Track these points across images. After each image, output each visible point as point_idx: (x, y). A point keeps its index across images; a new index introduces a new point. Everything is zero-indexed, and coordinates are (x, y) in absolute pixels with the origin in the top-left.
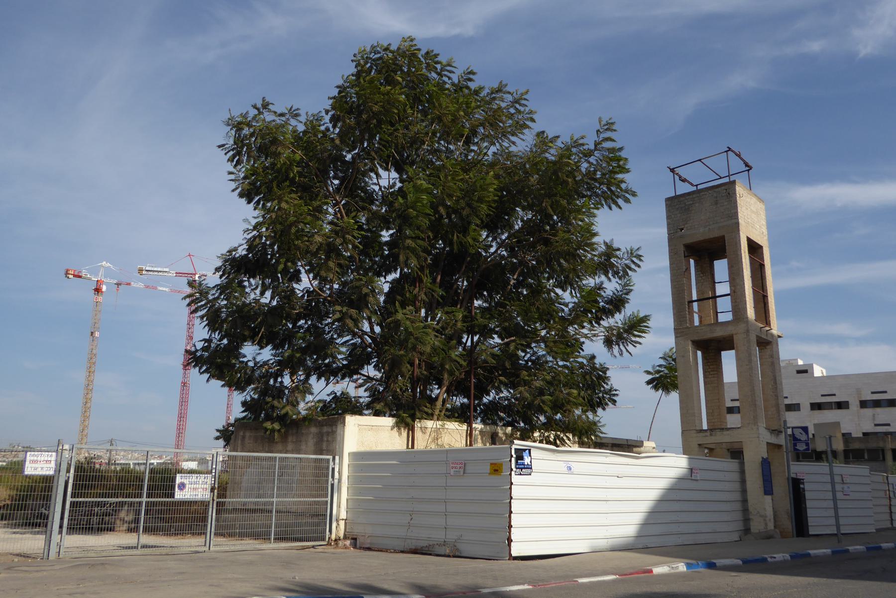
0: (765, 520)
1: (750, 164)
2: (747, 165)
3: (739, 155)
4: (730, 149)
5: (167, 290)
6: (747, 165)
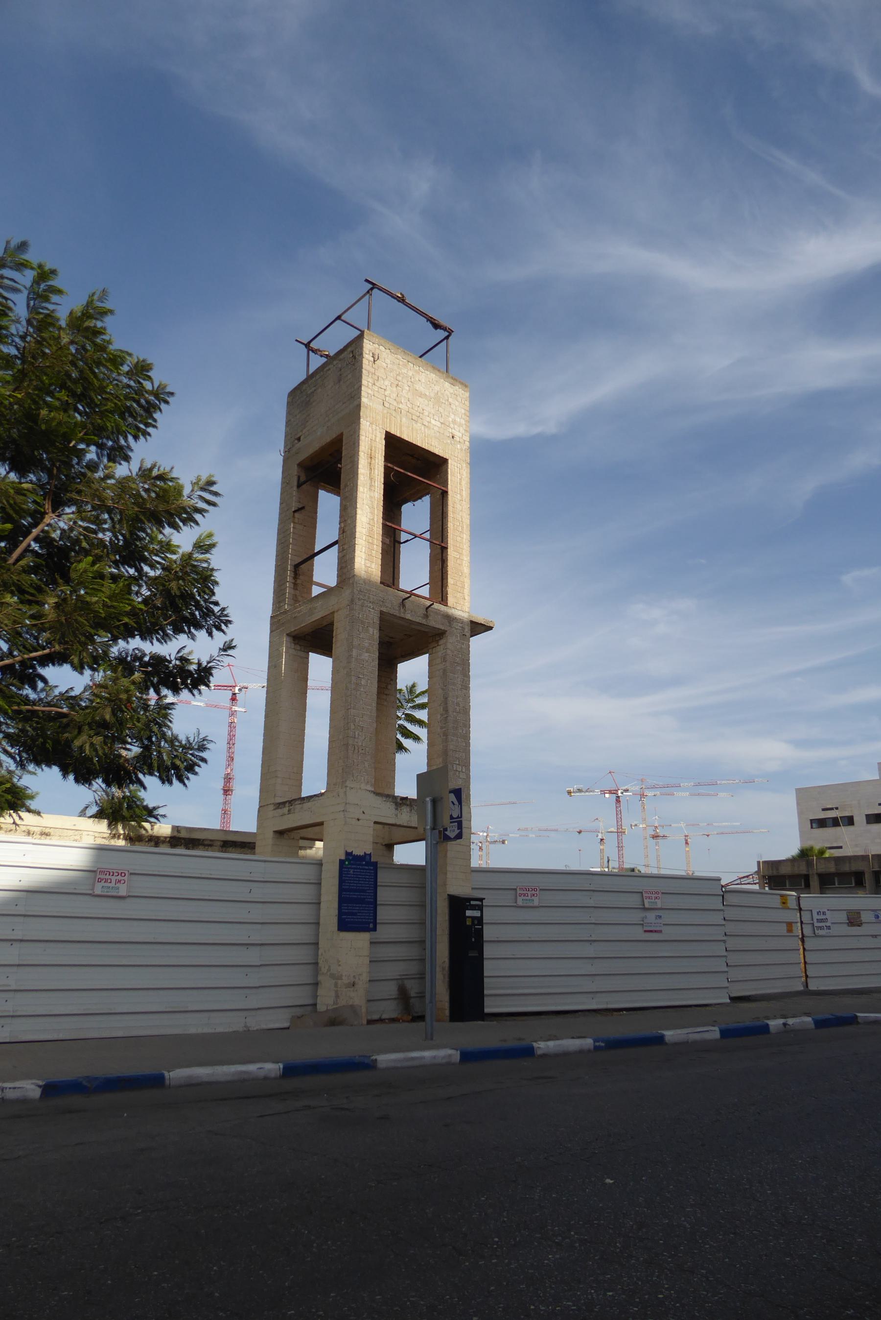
0: (336, 985)
1: (443, 322)
2: (436, 326)
3: (402, 300)
4: (374, 286)
6: (436, 326)
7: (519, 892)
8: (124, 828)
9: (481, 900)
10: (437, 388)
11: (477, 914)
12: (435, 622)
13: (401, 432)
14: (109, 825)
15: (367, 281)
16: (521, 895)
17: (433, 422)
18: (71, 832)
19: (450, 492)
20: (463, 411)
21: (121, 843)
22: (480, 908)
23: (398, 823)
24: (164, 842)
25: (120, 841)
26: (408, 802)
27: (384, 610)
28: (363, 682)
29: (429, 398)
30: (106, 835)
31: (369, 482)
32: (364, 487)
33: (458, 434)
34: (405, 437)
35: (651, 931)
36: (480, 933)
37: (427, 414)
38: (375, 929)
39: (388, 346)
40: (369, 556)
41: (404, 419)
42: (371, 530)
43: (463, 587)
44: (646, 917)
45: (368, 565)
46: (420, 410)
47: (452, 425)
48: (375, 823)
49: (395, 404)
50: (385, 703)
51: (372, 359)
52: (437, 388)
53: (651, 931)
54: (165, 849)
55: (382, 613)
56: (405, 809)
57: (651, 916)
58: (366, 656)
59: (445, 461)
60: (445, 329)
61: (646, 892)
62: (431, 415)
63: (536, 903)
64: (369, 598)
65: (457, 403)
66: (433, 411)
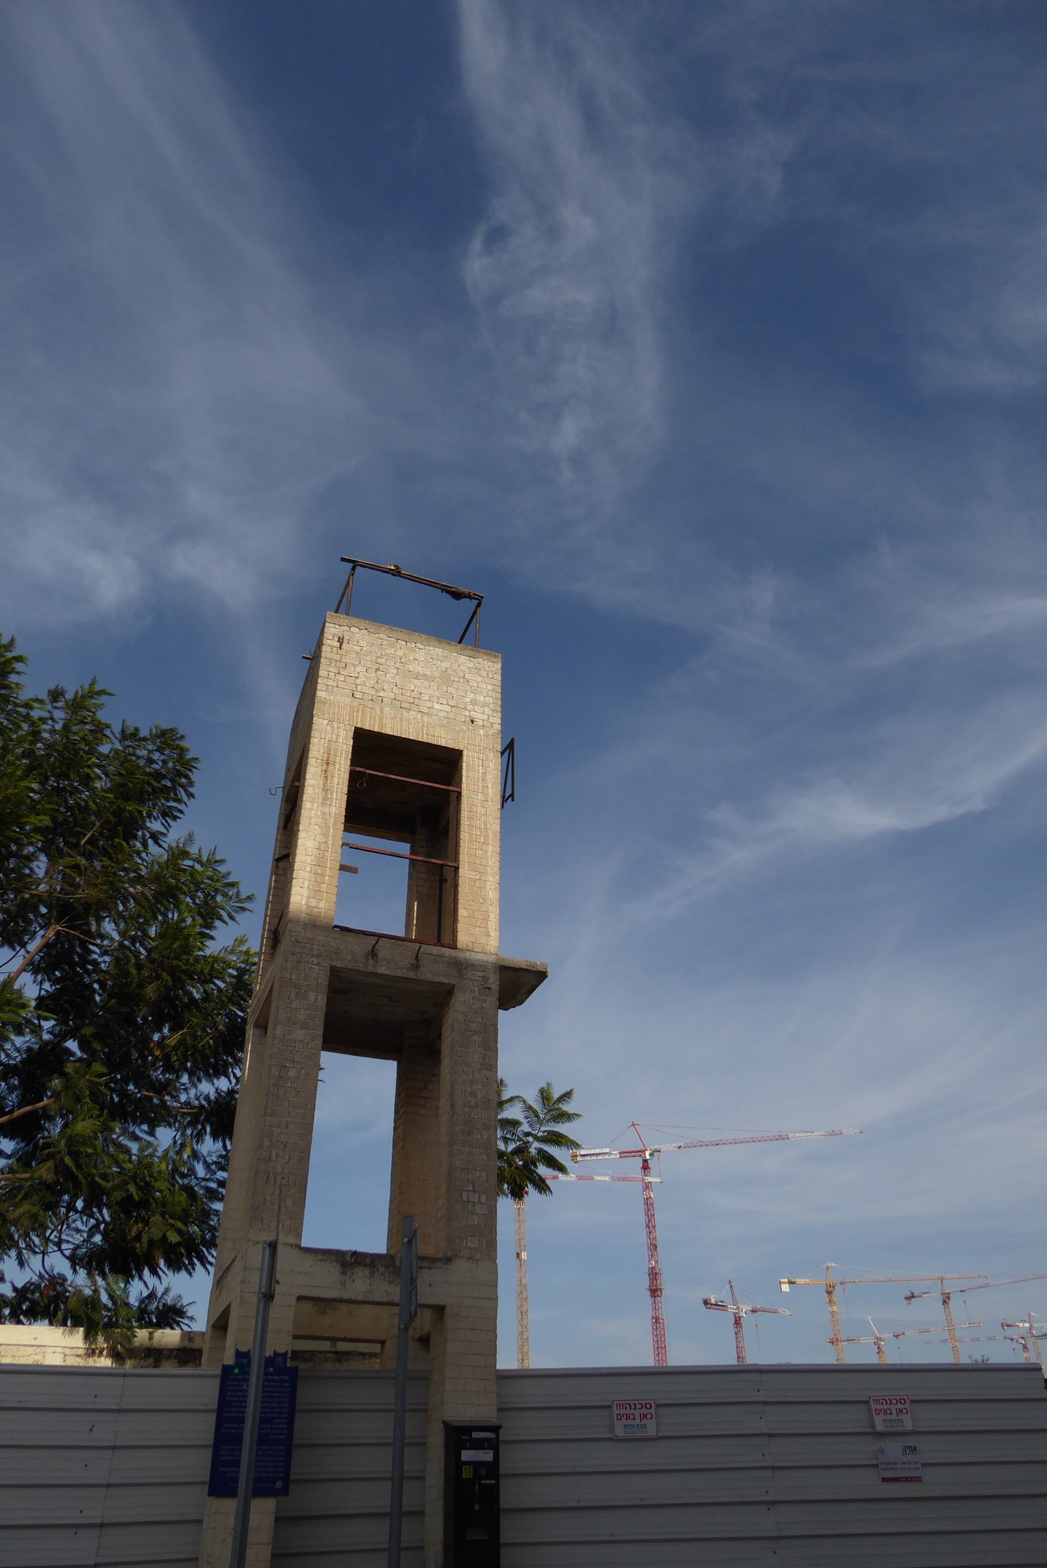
2: (457, 595)
3: (397, 573)
4: (355, 564)
5: (607, 1179)
6: (457, 595)
7: (616, 1411)
8: (106, 1340)
9: (496, 1429)
10: (445, 665)
11: (487, 1456)
12: (433, 973)
13: (381, 726)
14: (87, 1337)
15: (343, 559)
16: (620, 1417)
17: (437, 706)
18: (30, 1350)
19: (465, 793)
20: (490, 687)
21: (105, 1362)
22: (494, 1445)
23: (346, 1297)
24: (168, 1358)
25: (103, 1359)
26: (368, 1261)
27: (338, 964)
28: (292, 1073)
29: (432, 679)
30: (81, 1352)
31: (322, 794)
32: (312, 802)
33: (479, 716)
35: (897, 1480)
36: (492, 1495)
37: (427, 698)
38: (285, 1491)
39: (355, 621)
40: (316, 893)
41: (387, 709)
43: (487, 920)
44: (881, 1451)
45: (314, 904)
46: (415, 694)
47: (470, 707)
48: (300, 1298)
49: (373, 692)
51: (337, 644)
52: (445, 665)
53: (897, 1480)
54: (168, 1367)
55: (333, 970)
56: (361, 1273)
57: (893, 1449)
58: (300, 1034)
59: (458, 754)
60: (469, 596)
61: (876, 1401)
62: (434, 699)
63: (652, 1431)
64: (311, 949)
65: (480, 679)
66: (437, 694)
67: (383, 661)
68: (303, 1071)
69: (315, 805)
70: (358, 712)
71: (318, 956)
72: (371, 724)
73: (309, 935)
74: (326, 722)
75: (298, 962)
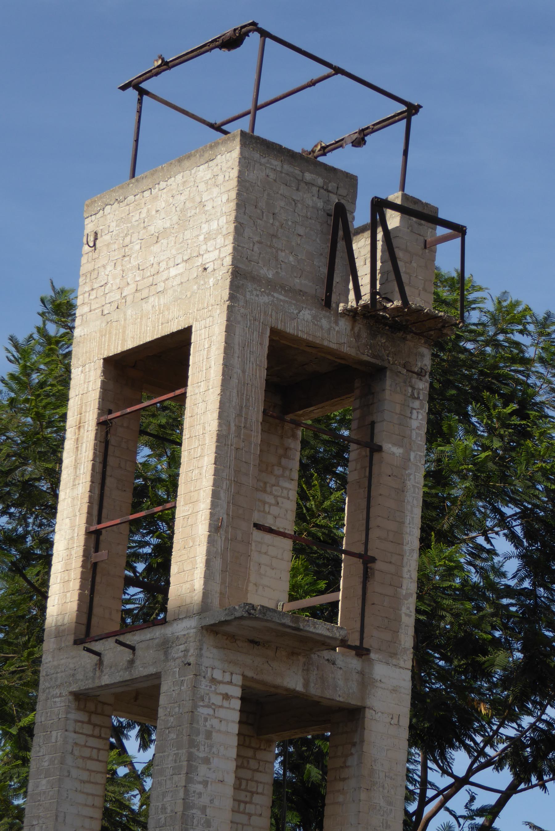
2: (232, 42)
3: (166, 65)
6: (232, 42)
15: (124, 88)
34: (130, 345)
41: (129, 312)
42: (69, 556)
50: (341, 799)
66: (174, 252)
67: (128, 239)
68: (44, 827)
69: (68, 491)
70: (105, 335)
71: (58, 686)
72: (116, 347)
73: (55, 663)
74: (80, 369)
75: (47, 699)
